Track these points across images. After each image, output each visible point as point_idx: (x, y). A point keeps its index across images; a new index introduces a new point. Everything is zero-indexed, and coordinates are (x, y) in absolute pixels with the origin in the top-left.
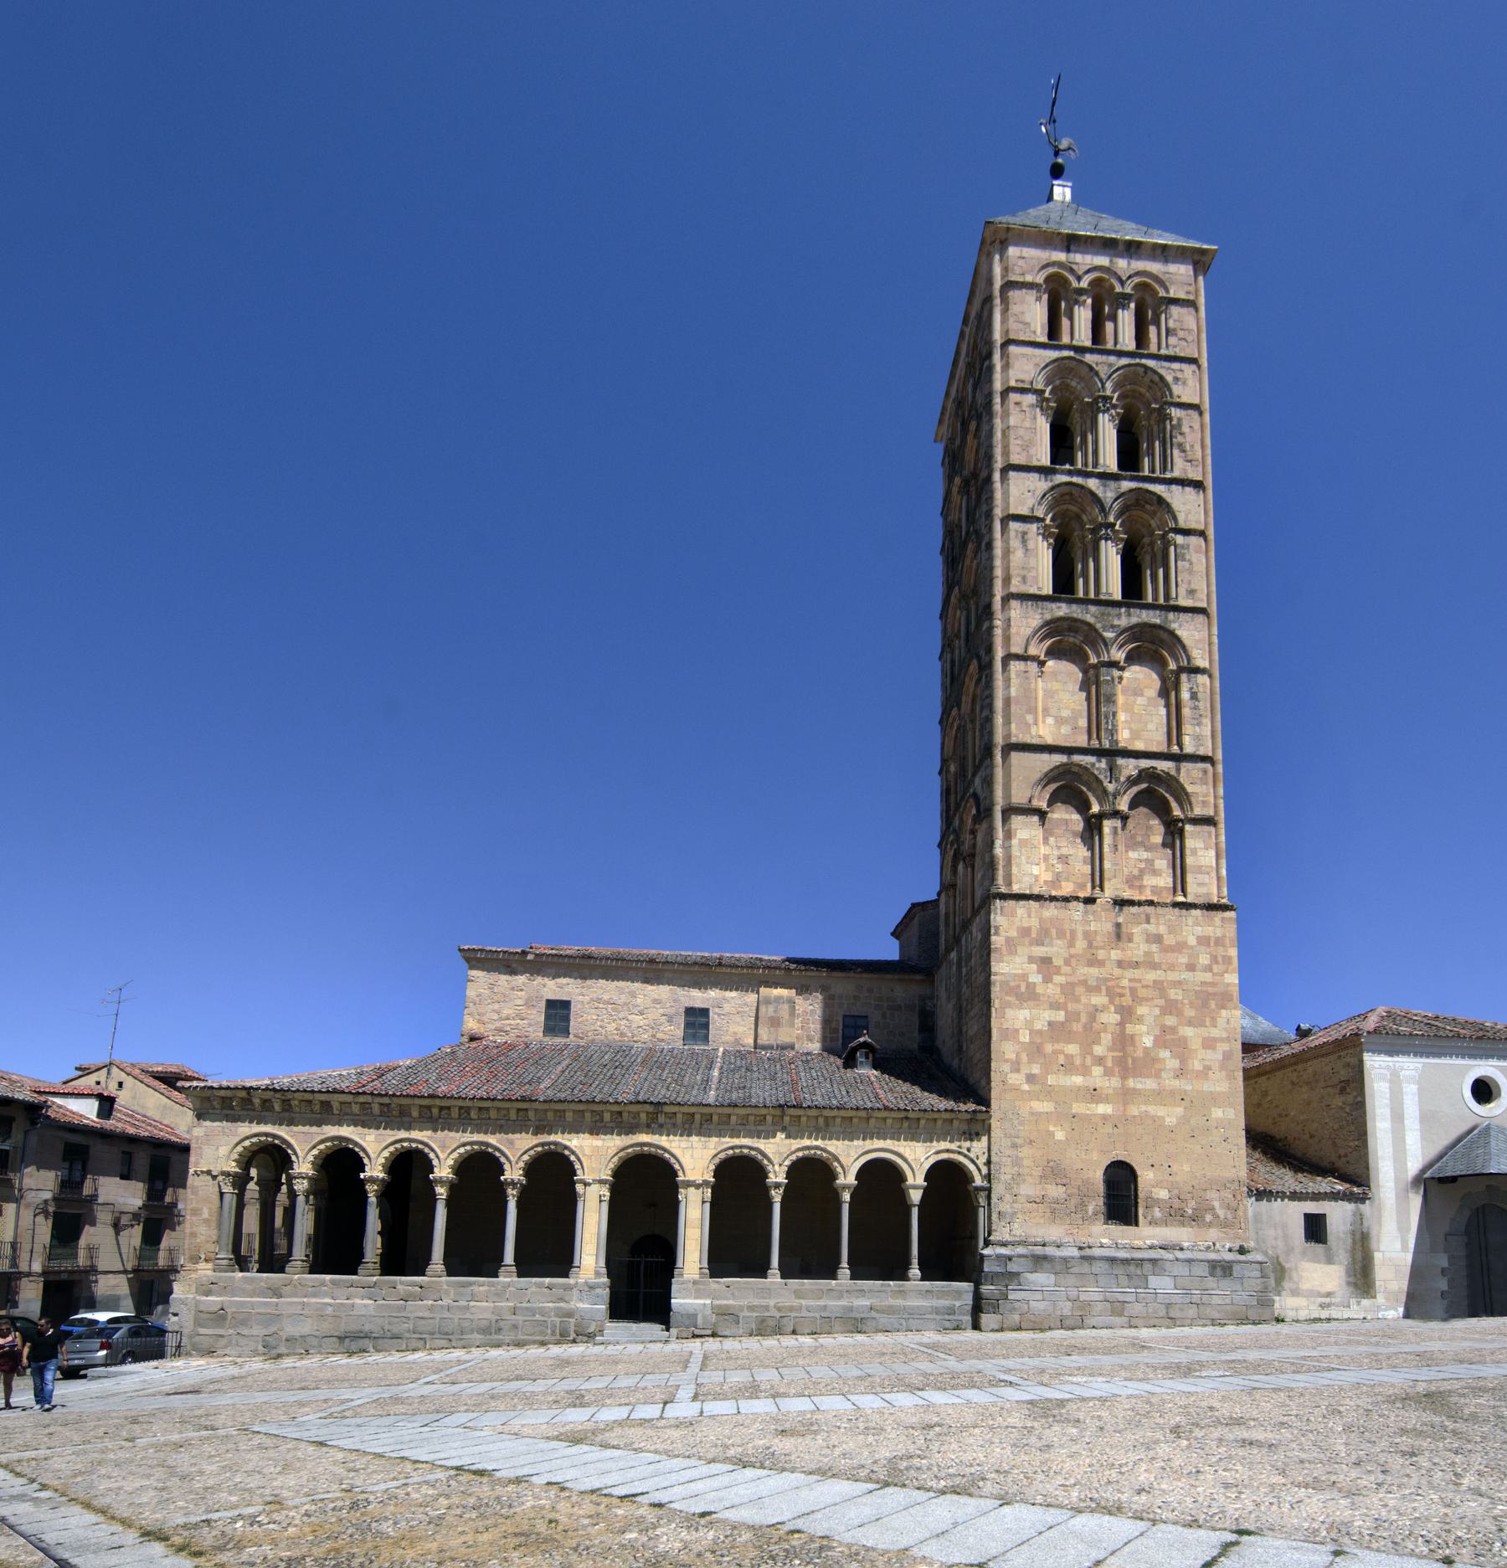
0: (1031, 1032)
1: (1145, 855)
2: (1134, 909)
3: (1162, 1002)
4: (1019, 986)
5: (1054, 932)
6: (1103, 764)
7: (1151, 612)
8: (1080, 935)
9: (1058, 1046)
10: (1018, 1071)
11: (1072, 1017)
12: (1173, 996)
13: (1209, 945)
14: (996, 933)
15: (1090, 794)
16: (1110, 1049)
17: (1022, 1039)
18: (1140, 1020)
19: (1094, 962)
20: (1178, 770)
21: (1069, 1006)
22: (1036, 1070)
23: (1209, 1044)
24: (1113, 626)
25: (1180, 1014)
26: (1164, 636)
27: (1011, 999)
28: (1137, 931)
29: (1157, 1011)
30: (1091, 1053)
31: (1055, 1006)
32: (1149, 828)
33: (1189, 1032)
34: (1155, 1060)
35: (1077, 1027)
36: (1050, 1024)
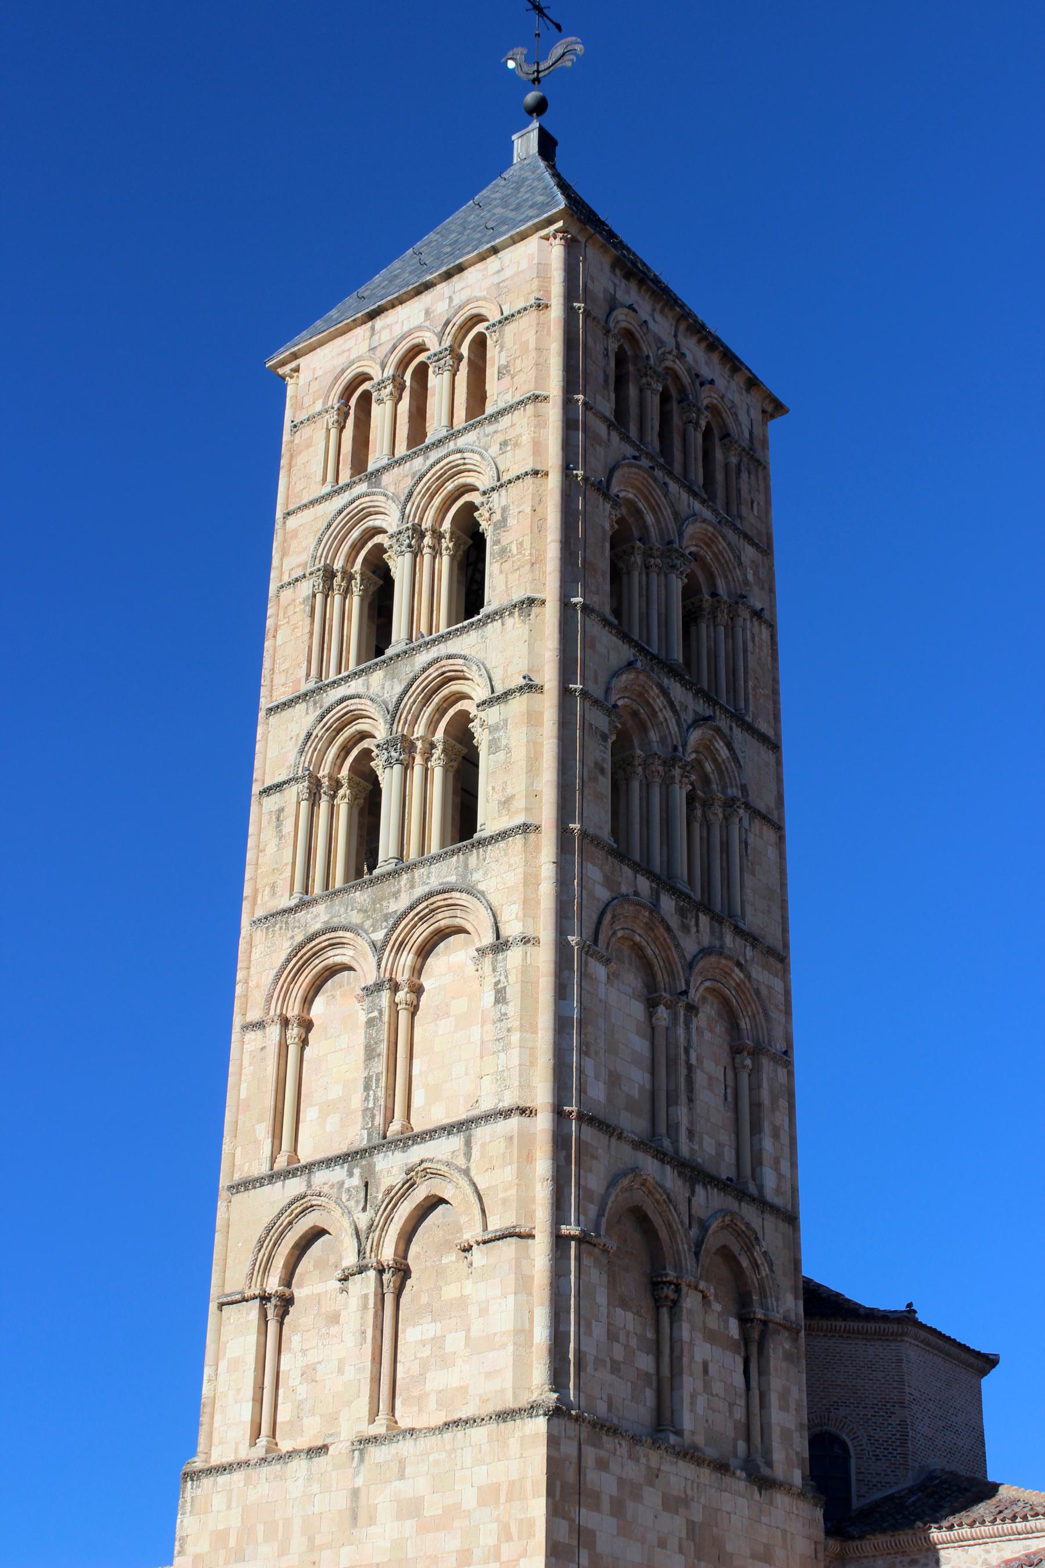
5: (260, 1528)
13: (497, 1502)
20: (468, 1155)
24: (386, 917)
28: (382, 1499)
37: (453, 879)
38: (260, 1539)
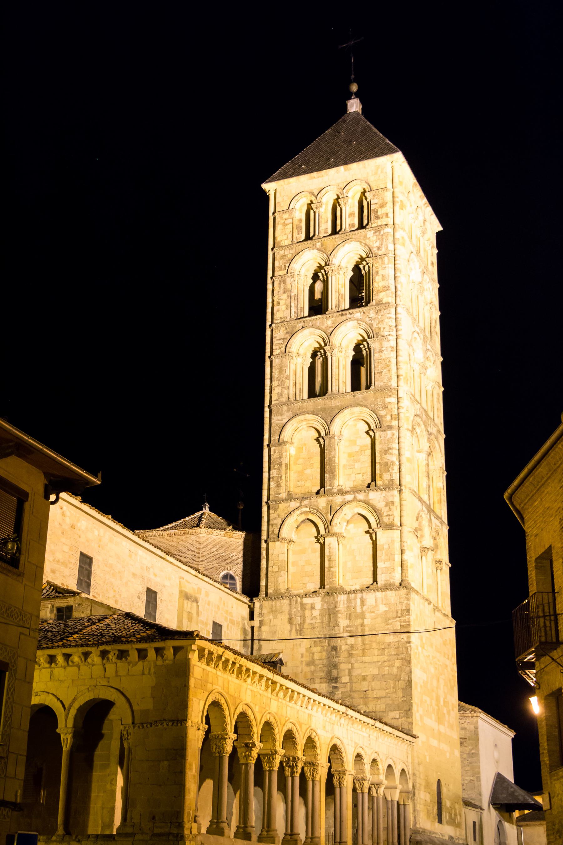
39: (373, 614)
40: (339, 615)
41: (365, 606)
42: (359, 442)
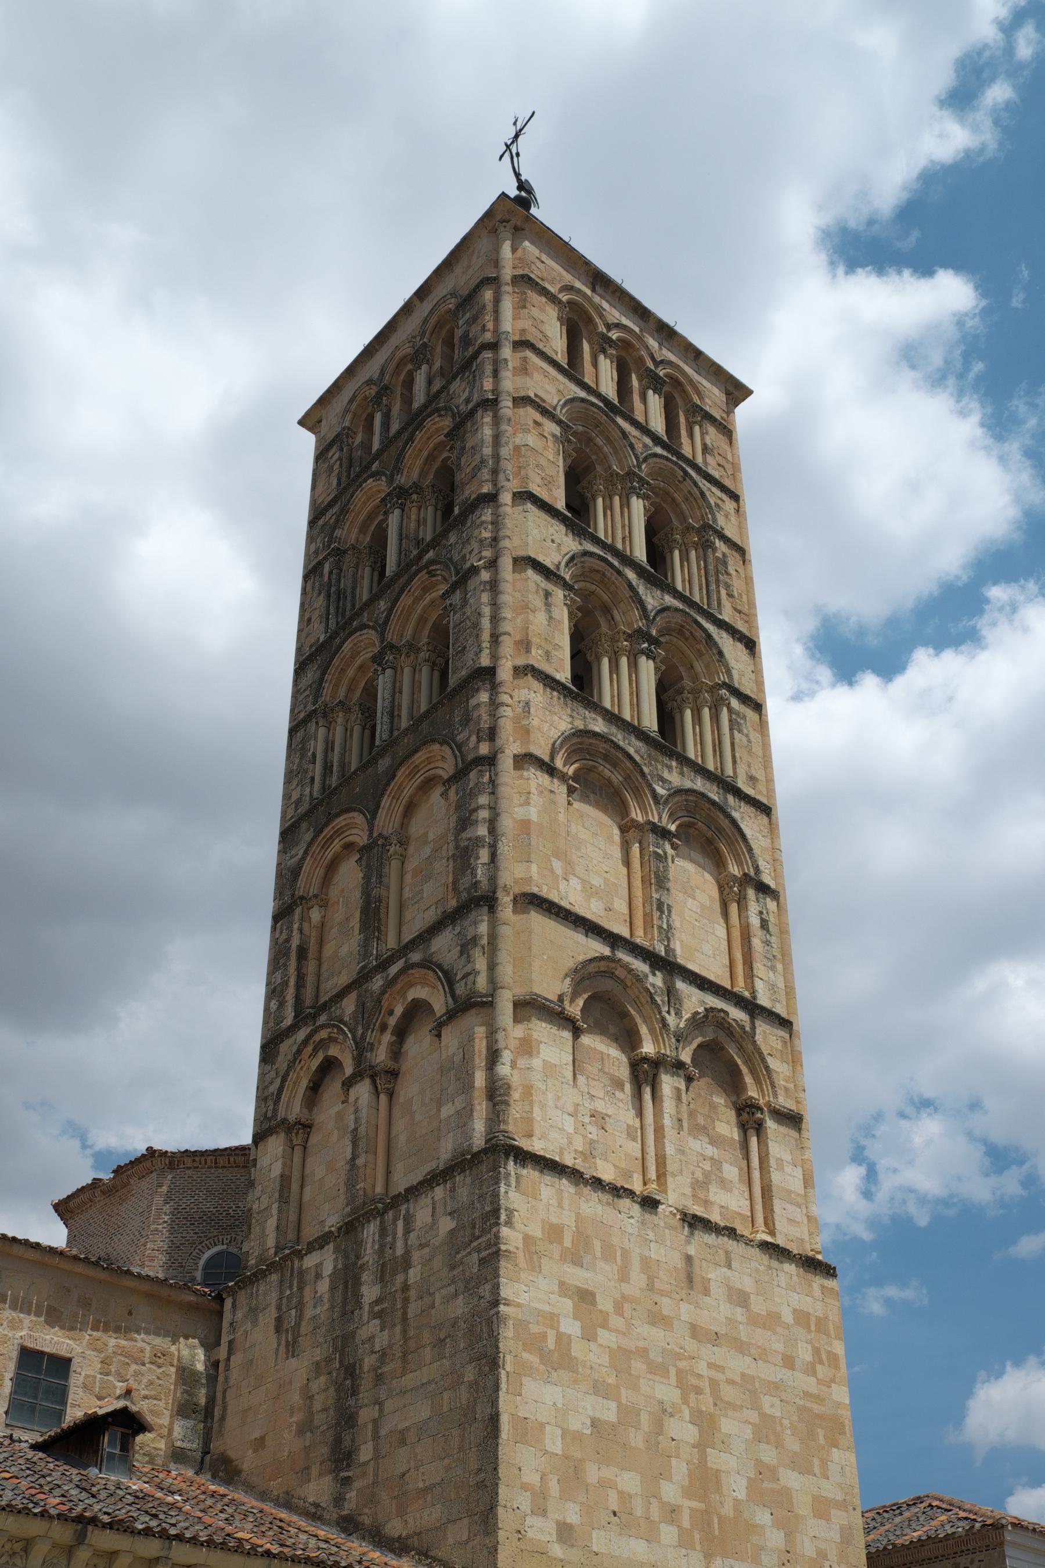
0: (565, 1432)
1: (710, 1151)
2: (710, 1239)
3: (753, 1416)
4: (544, 1336)
5: (597, 1245)
6: (657, 980)
7: (708, 785)
8: (635, 1263)
9: (609, 1473)
10: (544, 1513)
11: (628, 1415)
12: (768, 1410)
14: (509, 1223)
15: (639, 1020)
16: (688, 1493)
17: (550, 1447)
18: (725, 1444)
19: (657, 1319)
21: (623, 1391)
22: (572, 1515)
23: (822, 1508)
25: (779, 1445)
26: (725, 823)
27: (533, 1359)
29: (748, 1433)
30: (657, 1496)
31: (600, 1389)
32: (713, 1107)
33: (791, 1479)
34: (752, 1528)
35: (636, 1439)
36: (595, 1423)
37: (716, 798)
38: (598, 1254)
39: (427, 1250)
40: (365, 1277)
41: (412, 1235)
42: (431, 836)
